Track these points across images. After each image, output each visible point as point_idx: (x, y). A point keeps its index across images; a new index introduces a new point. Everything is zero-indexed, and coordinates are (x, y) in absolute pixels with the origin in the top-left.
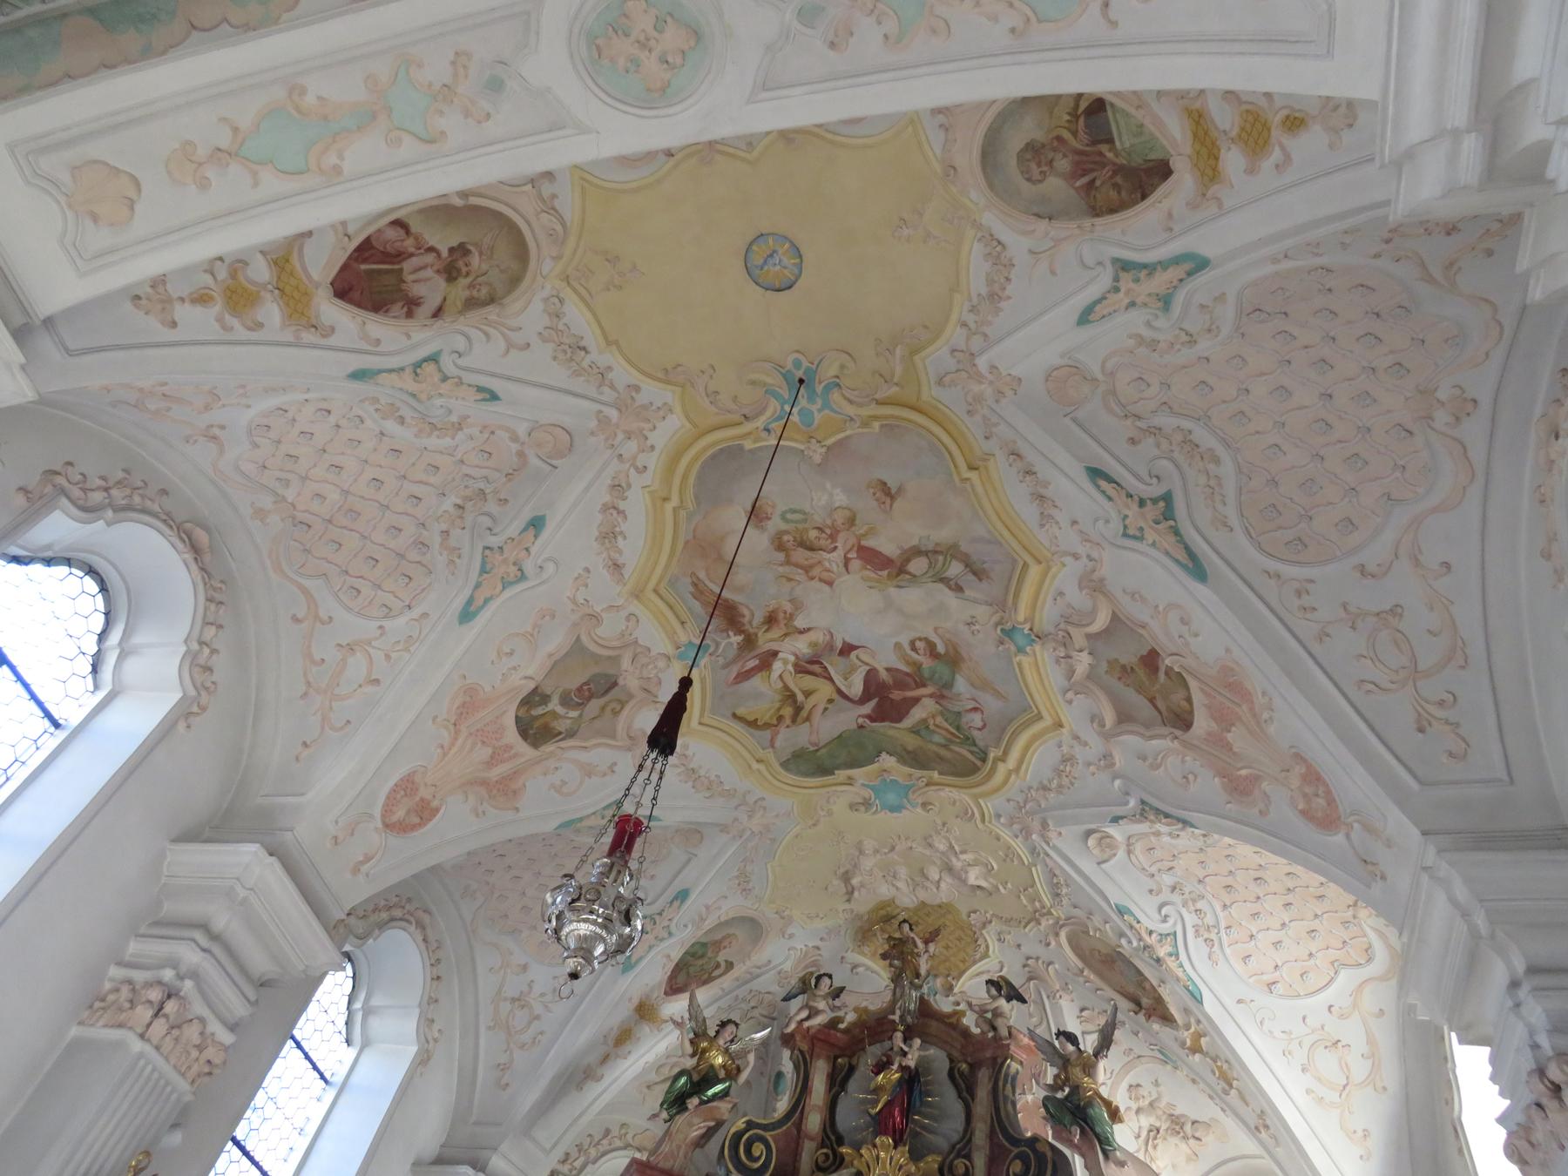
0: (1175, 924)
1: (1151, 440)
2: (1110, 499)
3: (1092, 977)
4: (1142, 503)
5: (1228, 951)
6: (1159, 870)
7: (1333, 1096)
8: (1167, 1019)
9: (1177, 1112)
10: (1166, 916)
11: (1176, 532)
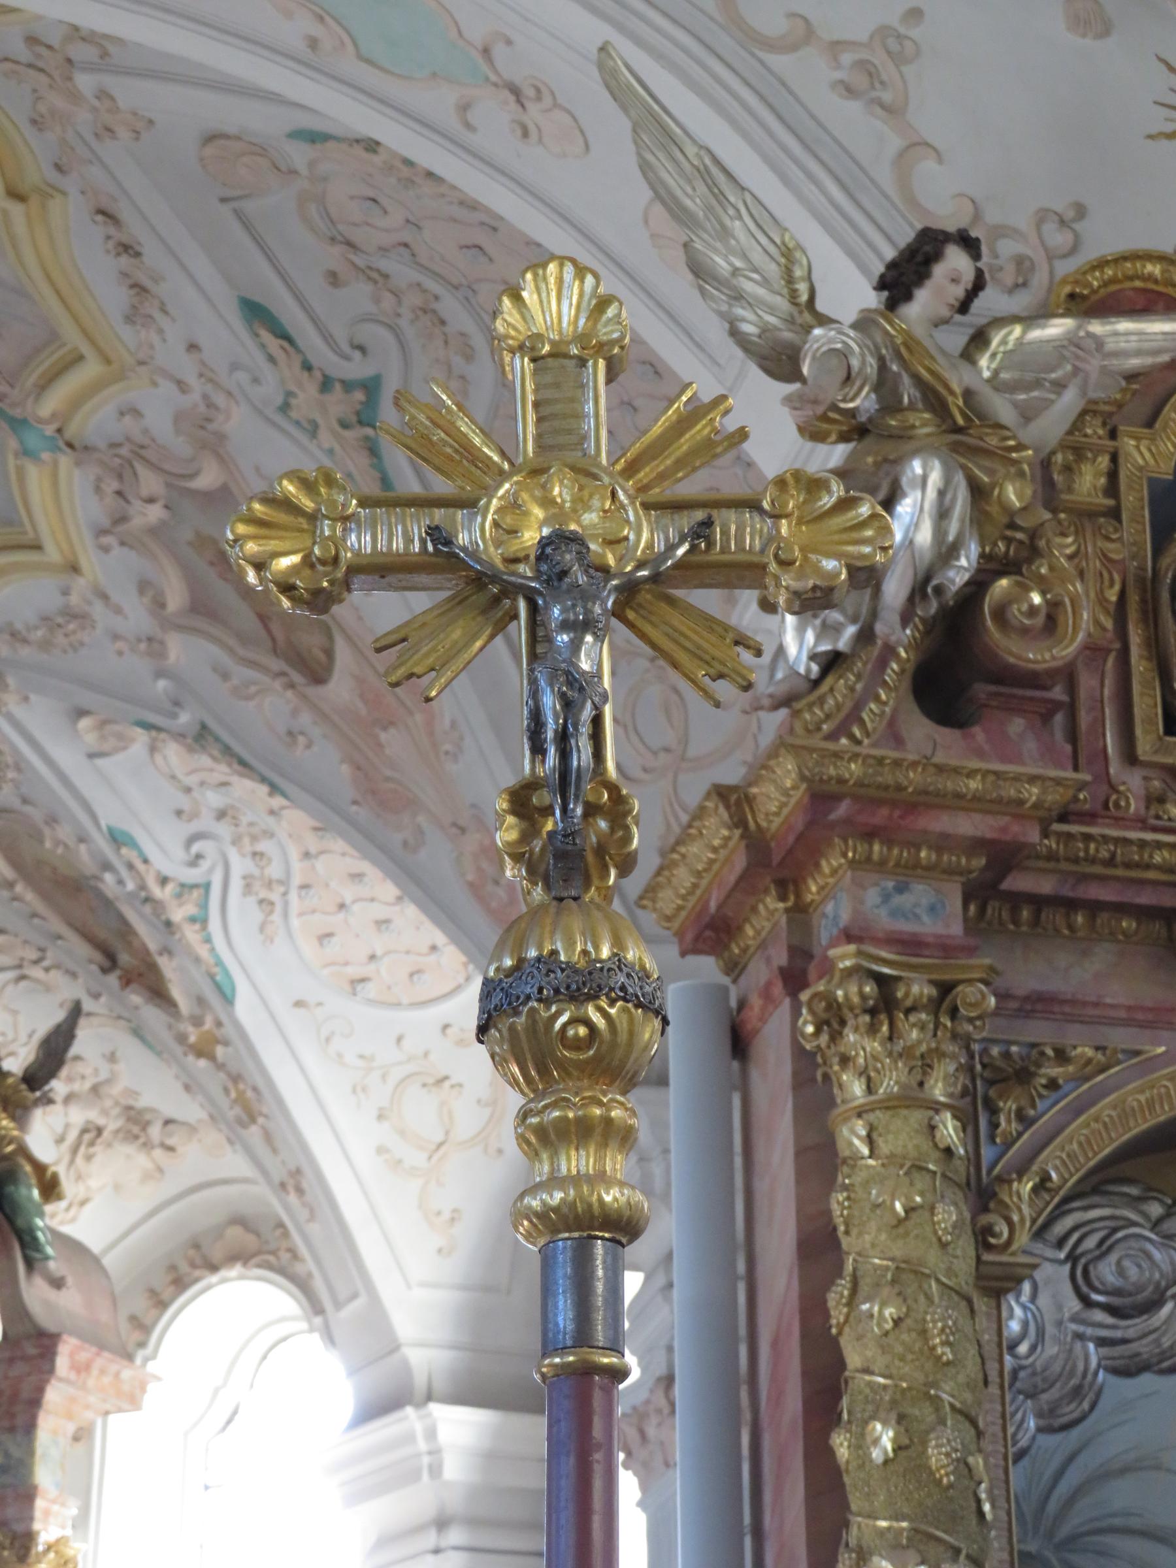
0: (211, 870)
1: (368, 288)
2: (272, 359)
3: (29, 896)
4: (326, 384)
5: (295, 922)
6: (202, 784)
7: (417, 1158)
8: (159, 994)
9: (141, 1103)
10: (199, 856)
11: (373, 450)
